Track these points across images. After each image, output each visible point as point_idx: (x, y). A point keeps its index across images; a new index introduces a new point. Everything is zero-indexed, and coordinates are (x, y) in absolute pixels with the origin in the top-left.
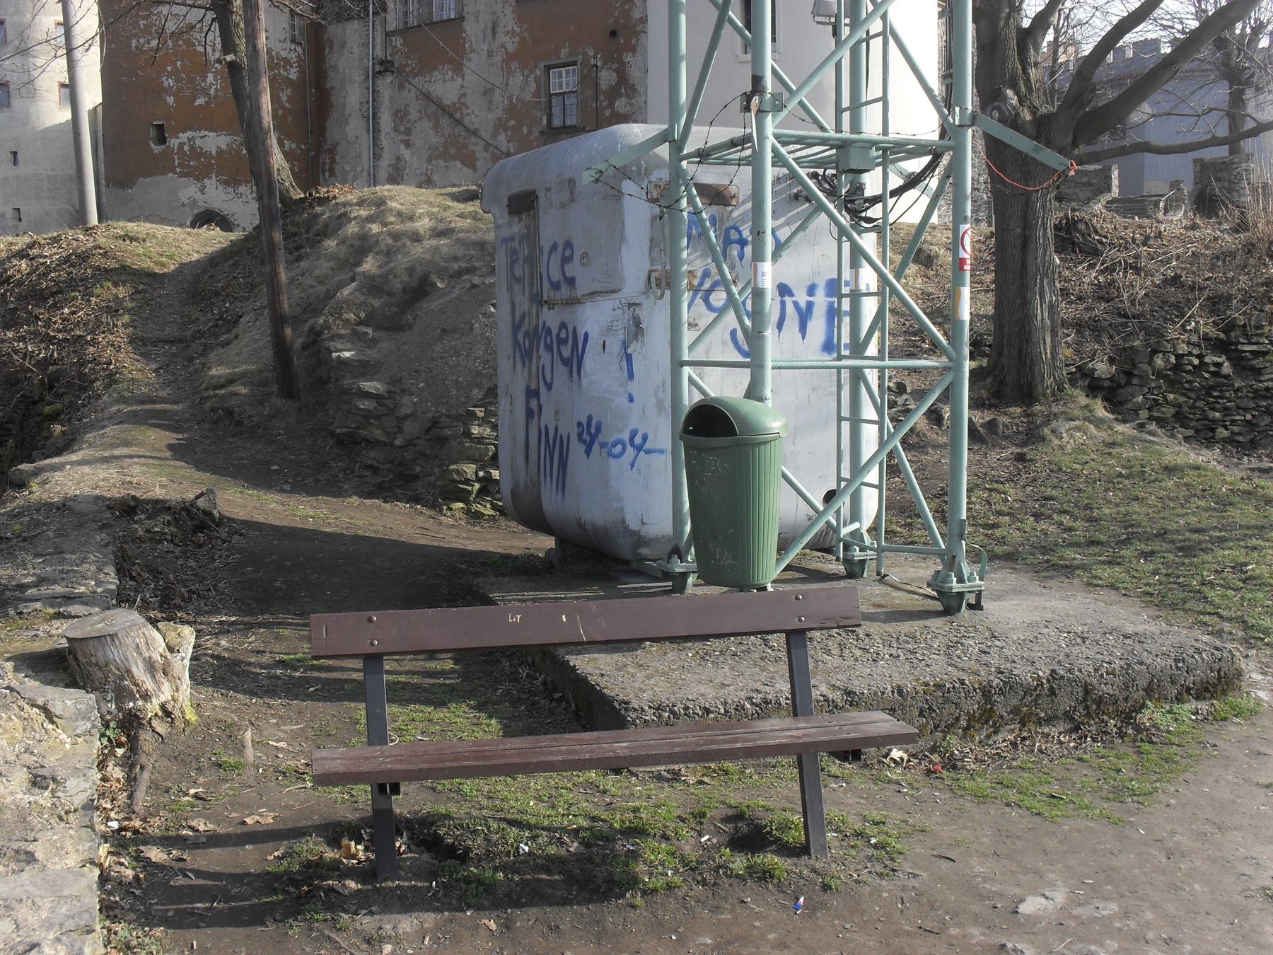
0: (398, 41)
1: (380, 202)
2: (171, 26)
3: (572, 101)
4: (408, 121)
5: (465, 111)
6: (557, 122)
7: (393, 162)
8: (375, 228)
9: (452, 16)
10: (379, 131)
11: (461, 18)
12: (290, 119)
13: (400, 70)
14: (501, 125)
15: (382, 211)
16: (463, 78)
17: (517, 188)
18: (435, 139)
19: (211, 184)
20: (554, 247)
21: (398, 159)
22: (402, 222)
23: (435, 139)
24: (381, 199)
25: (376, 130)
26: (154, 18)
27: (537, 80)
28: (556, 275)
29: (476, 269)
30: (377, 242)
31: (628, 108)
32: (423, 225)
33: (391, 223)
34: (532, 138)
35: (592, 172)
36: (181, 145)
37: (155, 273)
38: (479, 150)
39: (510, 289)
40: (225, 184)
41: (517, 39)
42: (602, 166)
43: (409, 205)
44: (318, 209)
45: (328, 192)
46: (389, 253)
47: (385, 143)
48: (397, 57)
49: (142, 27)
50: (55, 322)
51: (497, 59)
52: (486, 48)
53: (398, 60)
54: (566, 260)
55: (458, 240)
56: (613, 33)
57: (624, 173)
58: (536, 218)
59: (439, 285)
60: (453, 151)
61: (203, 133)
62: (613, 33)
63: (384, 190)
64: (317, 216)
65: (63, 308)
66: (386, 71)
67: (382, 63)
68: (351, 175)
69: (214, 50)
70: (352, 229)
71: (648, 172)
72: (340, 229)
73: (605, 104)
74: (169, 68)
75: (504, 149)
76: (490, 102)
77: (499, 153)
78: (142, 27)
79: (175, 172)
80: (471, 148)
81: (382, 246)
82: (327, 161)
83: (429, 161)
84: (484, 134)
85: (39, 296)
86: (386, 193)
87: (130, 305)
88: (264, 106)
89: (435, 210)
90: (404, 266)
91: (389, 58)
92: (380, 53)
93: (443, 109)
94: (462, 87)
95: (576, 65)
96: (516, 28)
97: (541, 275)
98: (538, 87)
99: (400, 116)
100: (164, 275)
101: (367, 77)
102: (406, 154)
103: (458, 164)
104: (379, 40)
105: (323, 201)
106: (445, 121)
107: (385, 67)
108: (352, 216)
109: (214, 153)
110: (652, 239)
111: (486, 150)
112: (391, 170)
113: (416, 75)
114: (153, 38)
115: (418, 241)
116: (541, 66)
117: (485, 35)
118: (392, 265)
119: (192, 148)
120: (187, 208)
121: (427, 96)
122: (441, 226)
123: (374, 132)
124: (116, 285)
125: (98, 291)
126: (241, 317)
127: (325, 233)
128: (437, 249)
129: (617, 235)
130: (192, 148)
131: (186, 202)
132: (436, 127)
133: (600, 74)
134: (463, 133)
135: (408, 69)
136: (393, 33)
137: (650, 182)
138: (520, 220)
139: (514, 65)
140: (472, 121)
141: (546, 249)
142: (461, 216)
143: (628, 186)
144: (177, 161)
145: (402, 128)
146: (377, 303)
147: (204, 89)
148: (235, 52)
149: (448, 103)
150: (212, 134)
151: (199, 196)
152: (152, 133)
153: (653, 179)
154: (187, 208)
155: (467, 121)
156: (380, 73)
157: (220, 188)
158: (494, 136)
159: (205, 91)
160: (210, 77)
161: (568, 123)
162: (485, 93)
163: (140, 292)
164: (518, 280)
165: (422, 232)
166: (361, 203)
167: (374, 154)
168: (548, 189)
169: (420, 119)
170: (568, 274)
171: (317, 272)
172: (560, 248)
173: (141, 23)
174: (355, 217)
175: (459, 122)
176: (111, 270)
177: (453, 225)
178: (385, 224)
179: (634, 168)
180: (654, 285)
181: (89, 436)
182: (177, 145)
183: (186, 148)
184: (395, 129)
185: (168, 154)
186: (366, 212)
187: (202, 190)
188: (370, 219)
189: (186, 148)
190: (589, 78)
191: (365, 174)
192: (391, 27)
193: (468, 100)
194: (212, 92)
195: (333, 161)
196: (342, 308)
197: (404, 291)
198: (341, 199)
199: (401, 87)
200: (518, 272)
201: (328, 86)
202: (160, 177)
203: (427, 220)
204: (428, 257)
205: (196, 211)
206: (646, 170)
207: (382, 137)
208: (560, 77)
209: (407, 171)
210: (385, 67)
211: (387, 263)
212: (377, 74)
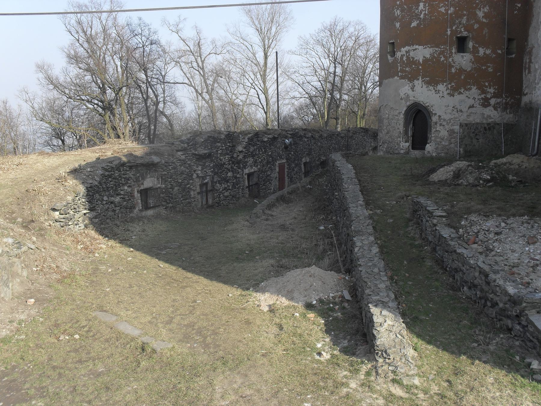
12: (486, 31)
19: (418, 83)
36: (402, 56)
40: (428, 83)
74: (398, 3)
79: (398, 76)
82: (528, 61)
109: (421, 61)
120: (403, 101)
130: (408, 58)
144: (399, 68)
151: (410, 92)
154: (403, 101)
157: (424, 86)
159: (417, 17)
182: (400, 56)
183: (405, 58)
185: (395, 61)
187: (413, 89)
194: (422, 16)
195: (530, 62)
202: (391, 80)
205: (408, 103)
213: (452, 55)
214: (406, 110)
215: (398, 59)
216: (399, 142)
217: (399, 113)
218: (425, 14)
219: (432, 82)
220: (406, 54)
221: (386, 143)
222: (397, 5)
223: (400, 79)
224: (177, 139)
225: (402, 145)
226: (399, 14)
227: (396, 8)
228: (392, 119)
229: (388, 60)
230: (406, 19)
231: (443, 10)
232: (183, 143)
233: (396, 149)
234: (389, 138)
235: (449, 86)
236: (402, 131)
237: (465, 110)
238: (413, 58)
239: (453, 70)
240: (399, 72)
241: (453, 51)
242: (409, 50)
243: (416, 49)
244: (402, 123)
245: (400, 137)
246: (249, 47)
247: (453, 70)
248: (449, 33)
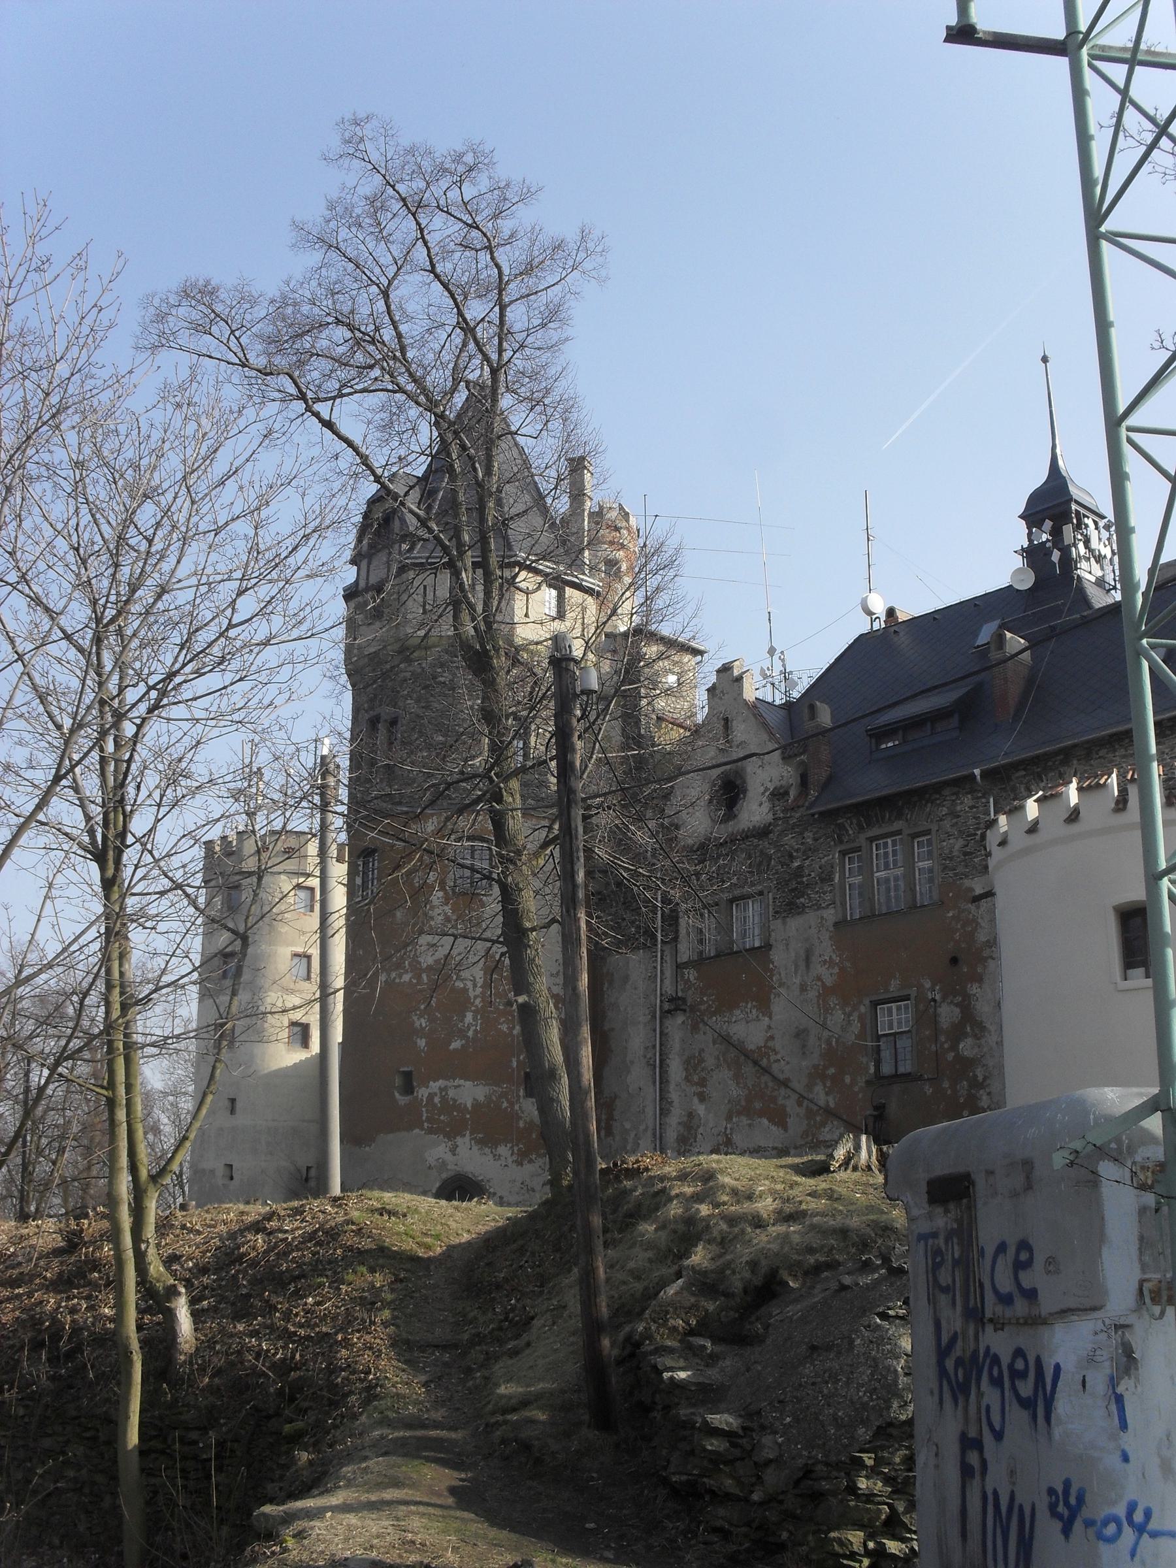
0: (691, 974)
1: (708, 1176)
2: (427, 960)
3: (904, 1043)
4: (703, 1070)
5: (772, 1058)
6: (887, 1069)
7: (685, 1119)
8: (704, 1210)
9: (757, 944)
10: (667, 1081)
11: (767, 946)
13: (693, 1009)
14: (817, 1074)
15: (711, 1188)
16: (771, 1018)
17: (939, 1171)
18: (735, 1091)
20: (1002, 1248)
21: (691, 1115)
22: (738, 1202)
23: (735, 1091)
24: (708, 1171)
25: (664, 1081)
27: (861, 1018)
28: (1005, 1283)
29: (839, 1264)
30: (708, 1227)
31: (976, 1050)
32: (766, 1206)
33: (724, 1204)
34: (856, 1089)
35: (1066, 1153)
36: (431, 1097)
37: (419, 1257)
38: (791, 1105)
39: (932, 1301)
40: (482, 1143)
41: (836, 970)
42: (1077, 1145)
43: (745, 1182)
44: (628, 1184)
45: (637, 1161)
46: (724, 1242)
47: (674, 1095)
48: (690, 992)
50: (297, 1315)
51: (812, 994)
52: (798, 981)
53: (691, 997)
54: (1020, 1266)
55: (813, 1227)
56: (954, 961)
57: (1101, 1152)
58: (971, 1208)
59: (791, 1284)
60: (758, 1105)
61: (457, 1082)
62: (954, 961)
63: (712, 1161)
64: (625, 1193)
65: (306, 1297)
66: (676, 1010)
67: (671, 1000)
68: (632, 1135)
69: (475, 986)
70: (674, 1210)
71: (1131, 1150)
72: (657, 1209)
73: (946, 1046)
75: (822, 1103)
76: (804, 1046)
77: (815, 1108)
79: (422, 1129)
80: (780, 1101)
81: (715, 1233)
83: (729, 1118)
84: (795, 1084)
85: (279, 1281)
86: (714, 1165)
87: (389, 1297)
88: (584, 1061)
89: (779, 1187)
90: (744, 1259)
91: (680, 994)
92: (669, 989)
93: (746, 1054)
94: (769, 1027)
95: (908, 999)
96: (834, 957)
97: (981, 1286)
98: (863, 1026)
99: (693, 1064)
100: (429, 1258)
101: (654, 1017)
102: (701, 1109)
103: (765, 1121)
104: (668, 973)
105: (634, 1173)
106: (748, 1069)
107: (675, 1005)
108: (673, 1193)
109: (469, 1105)
110: (1141, 1238)
111: (800, 1104)
112: (681, 1128)
113: (714, 1014)
114: (407, 972)
115: (760, 1227)
116: (867, 1002)
117: (797, 967)
118: (728, 1257)
119: (444, 1099)
121: (726, 1039)
122: (788, 1208)
123: (661, 1083)
124: (372, 1270)
125: (350, 1277)
126: (532, 1318)
127: (638, 1213)
128: (786, 1237)
129: (1096, 1235)
130: (444, 1099)
132: (737, 1077)
133: (939, 1010)
134: (770, 1084)
135: (703, 1007)
136: (686, 965)
137: (1134, 1163)
138: (947, 1211)
139: (833, 1001)
140: (781, 1069)
141: (990, 1251)
142: (813, 1194)
143: (1107, 1169)
145: (696, 1078)
146: (711, 1306)
147: (460, 1031)
148: (529, 993)
149: (752, 1047)
150: (468, 1084)
151: (449, 1157)
152: (398, 1081)
153: (1138, 1158)
155: (775, 1068)
156: (669, 1012)
157: (475, 1148)
158: (810, 1087)
159: (462, 1033)
160: (469, 1017)
161: (901, 1070)
162: (797, 1035)
163: (401, 1281)
164: (946, 1290)
165: (765, 1216)
166: (683, 1177)
167: (661, 1109)
168: (990, 1173)
169: (718, 1066)
170: (1026, 1284)
171: (631, 1265)
172: (1011, 1251)
174: (677, 1196)
175: (766, 1071)
176: (367, 1251)
177: (804, 1207)
178: (717, 1205)
179: (1113, 1145)
180: (1148, 1300)
181: (347, 1470)
182: (426, 1095)
183: (437, 1100)
184: (687, 1079)
186: (692, 1189)
187: (453, 1150)
188: (698, 1198)
189: (437, 1100)
190: (926, 1016)
191: (649, 1133)
192: (684, 957)
193: (777, 1044)
194: (470, 1034)
196: (667, 1312)
197: (745, 1291)
198: (657, 1172)
199: (695, 1028)
200: (944, 1278)
201: (607, 1027)
203: (770, 1200)
204: (775, 1247)
205: (444, 1176)
206: (1129, 1147)
207: (672, 1087)
208: (890, 1014)
209: (701, 1130)
210: (675, 1005)
211: (721, 1256)
212: (666, 1013)
213: (518, 1100)
218: (476, 1030)
219: (488, 1140)
231: (504, 1028)
235: (516, 1149)
237: (538, 1188)
238: (455, 1101)
239: (521, 1124)
241: (522, 1093)
243: (459, 1086)
247: (521, 1124)
248: (515, 1064)
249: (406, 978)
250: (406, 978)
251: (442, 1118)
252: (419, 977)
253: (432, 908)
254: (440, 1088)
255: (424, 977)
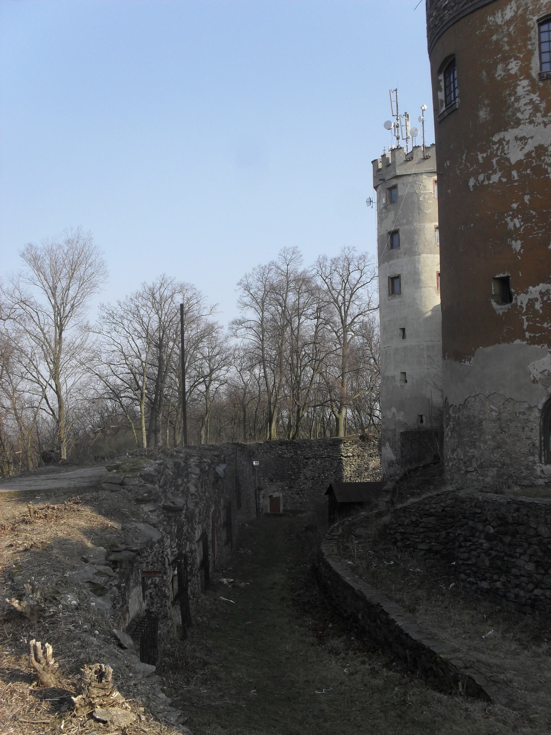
26: (495, 147)
36: (532, 302)
49: (481, 161)
74: (515, 206)
78: (481, 161)
79: (523, 338)
114: (495, 172)
120: (540, 386)
131: (538, 377)
144: (526, 324)
152: (494, 289)
154: (540, 386)
173: (480, 157)
182: (525, 302)
183: (538, 306)
189: (538, 306)
202: (503, 346)
214: (547, 402)
215: (521, 307)
216: (530, 464)
217: (530, 408)
220: (542, 298)
221: (496, 466)
222: (513, 210)
223: (530, 344)
224: (132, 470)
225: (539, 470)
226: (518, 225)
227: (509, 215)
228: (511, 421)
229: (494, 311)
230: (538, 234)
232: (152, 482)
233: (525, 478)
234: (501, 456)
236: (537, 443)
240: (526, 331)
242: (548, 291)
244: (538, 427)
245: (533, 454)
246: (34, 314)
249: (495, 178)
250: (495, 178)
251: (545, 325)
252: (509, 176)
253: (518, 99)
254: (541, 293)
255: (514, 173)
